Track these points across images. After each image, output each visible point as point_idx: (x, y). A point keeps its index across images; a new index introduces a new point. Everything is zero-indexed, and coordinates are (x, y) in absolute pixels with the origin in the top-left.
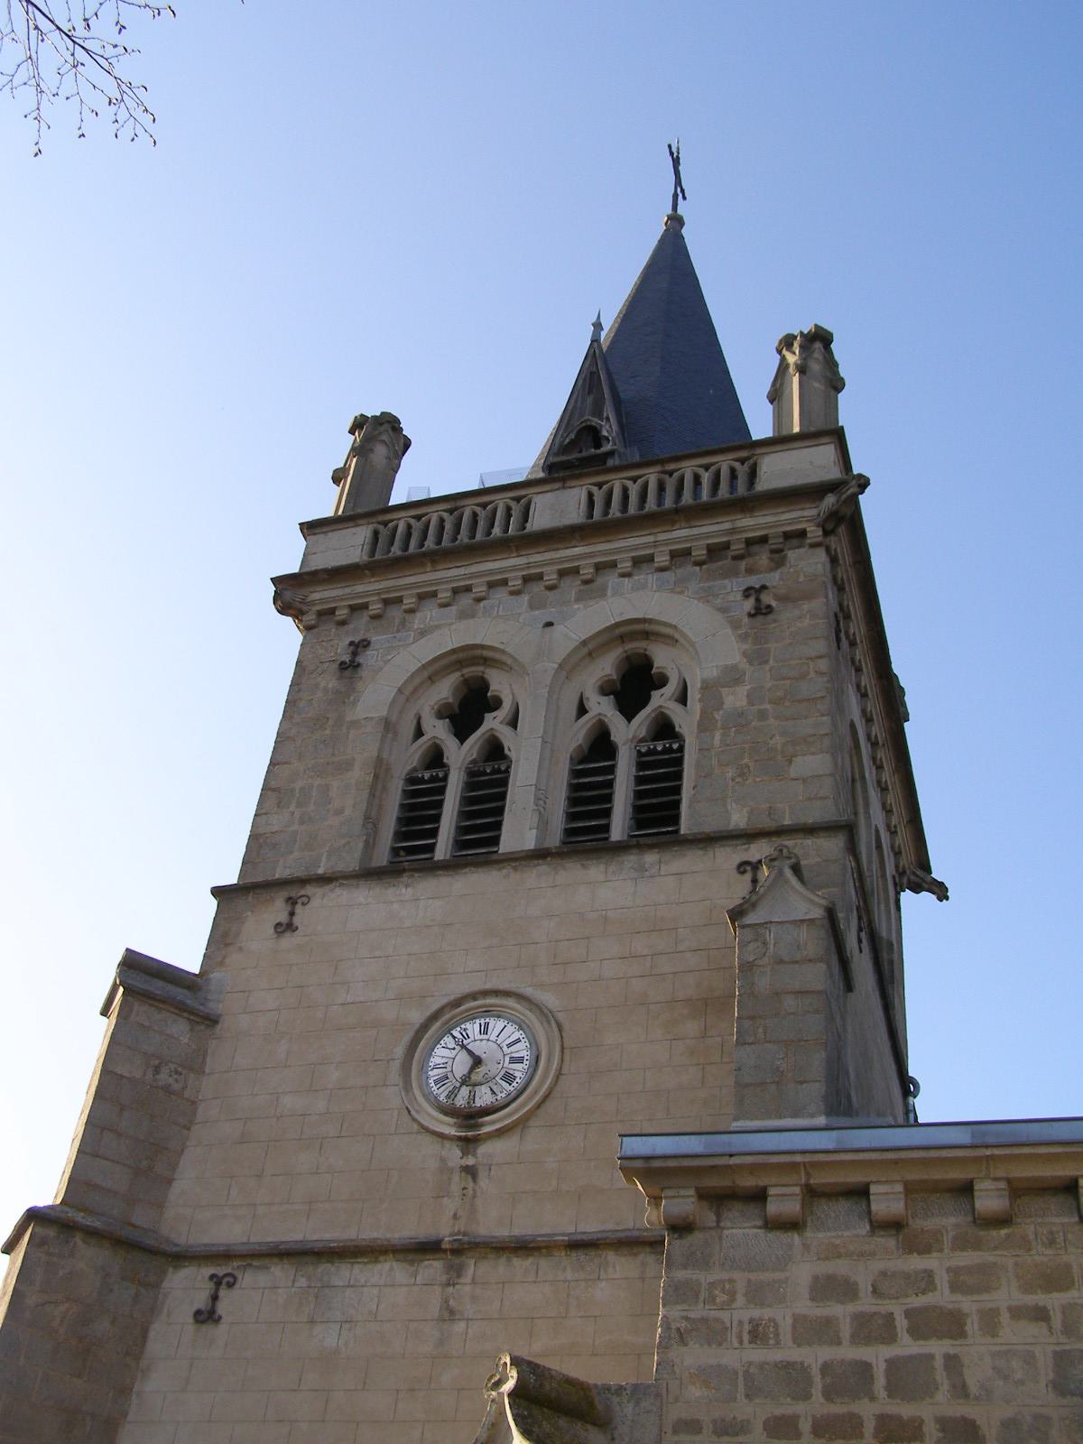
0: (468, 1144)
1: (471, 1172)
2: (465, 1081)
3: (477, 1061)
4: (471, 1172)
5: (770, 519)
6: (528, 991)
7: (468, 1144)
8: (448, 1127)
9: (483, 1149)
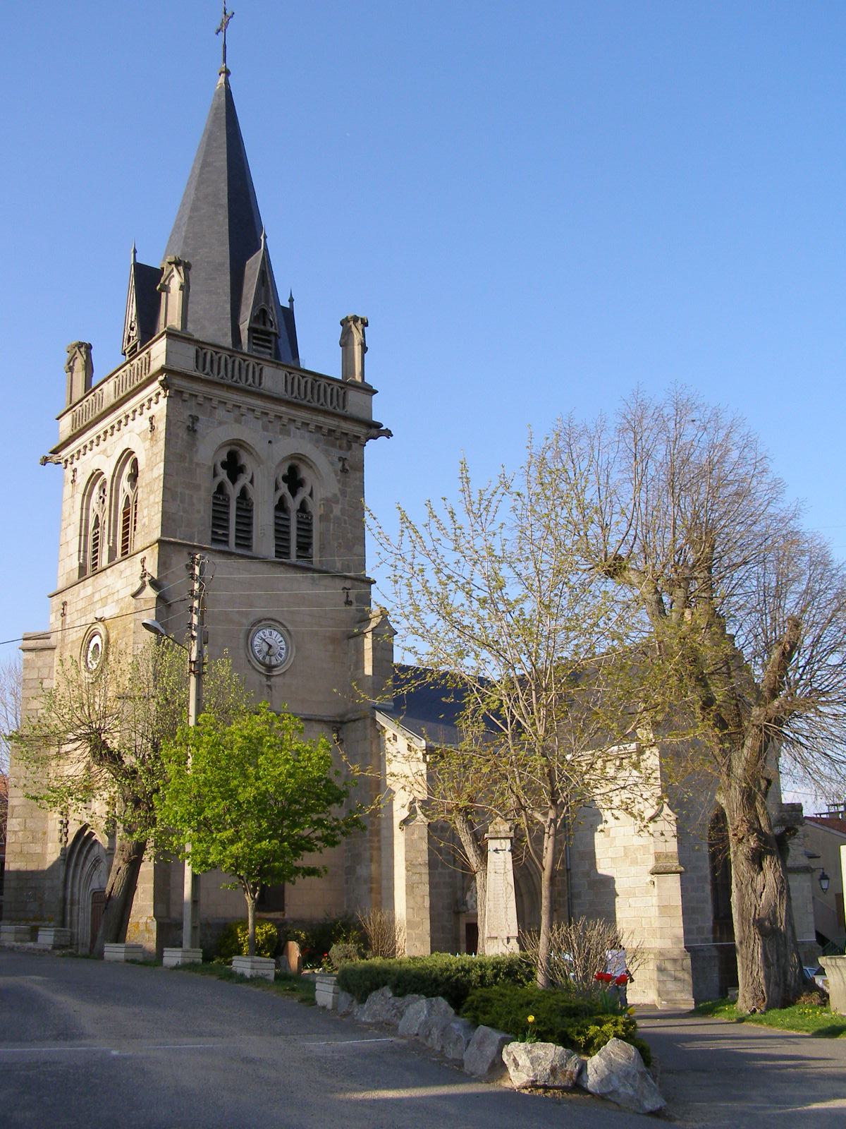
0: (269, 677)
1: (269, 686)
2: (268, 653)
3: (270, 646)
4: (269, 686)
5: (350, 427)
6: (281, 621)
7: (269, 677)
8: (262, 669)
9: (272, 679)
